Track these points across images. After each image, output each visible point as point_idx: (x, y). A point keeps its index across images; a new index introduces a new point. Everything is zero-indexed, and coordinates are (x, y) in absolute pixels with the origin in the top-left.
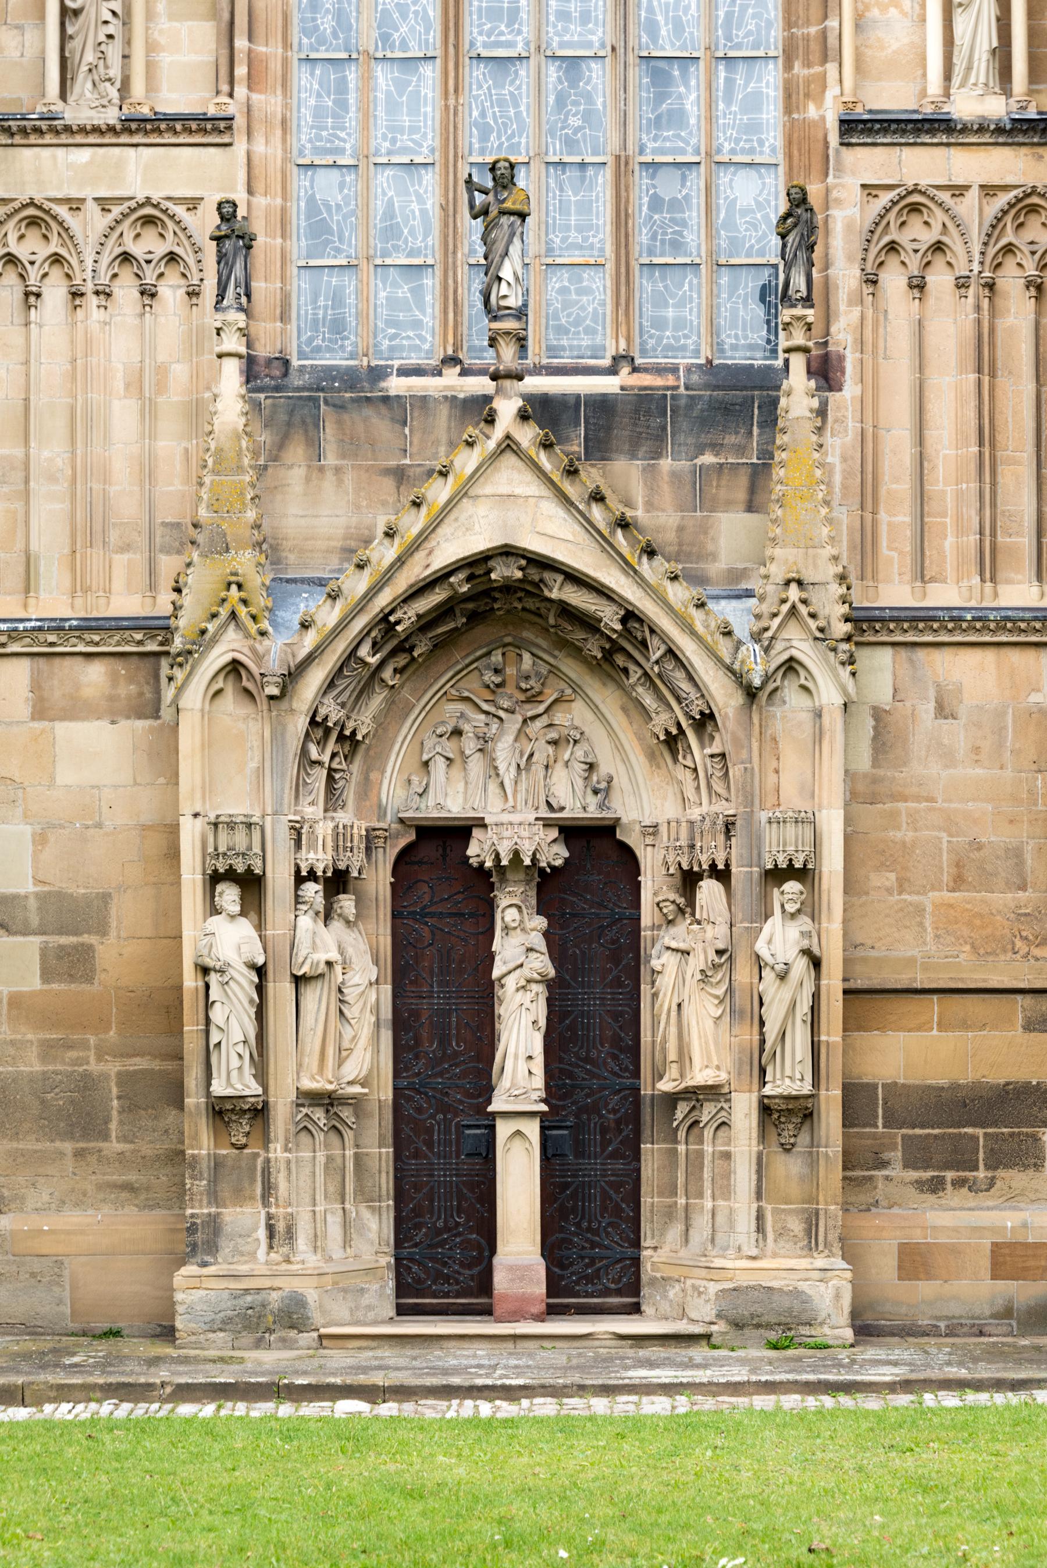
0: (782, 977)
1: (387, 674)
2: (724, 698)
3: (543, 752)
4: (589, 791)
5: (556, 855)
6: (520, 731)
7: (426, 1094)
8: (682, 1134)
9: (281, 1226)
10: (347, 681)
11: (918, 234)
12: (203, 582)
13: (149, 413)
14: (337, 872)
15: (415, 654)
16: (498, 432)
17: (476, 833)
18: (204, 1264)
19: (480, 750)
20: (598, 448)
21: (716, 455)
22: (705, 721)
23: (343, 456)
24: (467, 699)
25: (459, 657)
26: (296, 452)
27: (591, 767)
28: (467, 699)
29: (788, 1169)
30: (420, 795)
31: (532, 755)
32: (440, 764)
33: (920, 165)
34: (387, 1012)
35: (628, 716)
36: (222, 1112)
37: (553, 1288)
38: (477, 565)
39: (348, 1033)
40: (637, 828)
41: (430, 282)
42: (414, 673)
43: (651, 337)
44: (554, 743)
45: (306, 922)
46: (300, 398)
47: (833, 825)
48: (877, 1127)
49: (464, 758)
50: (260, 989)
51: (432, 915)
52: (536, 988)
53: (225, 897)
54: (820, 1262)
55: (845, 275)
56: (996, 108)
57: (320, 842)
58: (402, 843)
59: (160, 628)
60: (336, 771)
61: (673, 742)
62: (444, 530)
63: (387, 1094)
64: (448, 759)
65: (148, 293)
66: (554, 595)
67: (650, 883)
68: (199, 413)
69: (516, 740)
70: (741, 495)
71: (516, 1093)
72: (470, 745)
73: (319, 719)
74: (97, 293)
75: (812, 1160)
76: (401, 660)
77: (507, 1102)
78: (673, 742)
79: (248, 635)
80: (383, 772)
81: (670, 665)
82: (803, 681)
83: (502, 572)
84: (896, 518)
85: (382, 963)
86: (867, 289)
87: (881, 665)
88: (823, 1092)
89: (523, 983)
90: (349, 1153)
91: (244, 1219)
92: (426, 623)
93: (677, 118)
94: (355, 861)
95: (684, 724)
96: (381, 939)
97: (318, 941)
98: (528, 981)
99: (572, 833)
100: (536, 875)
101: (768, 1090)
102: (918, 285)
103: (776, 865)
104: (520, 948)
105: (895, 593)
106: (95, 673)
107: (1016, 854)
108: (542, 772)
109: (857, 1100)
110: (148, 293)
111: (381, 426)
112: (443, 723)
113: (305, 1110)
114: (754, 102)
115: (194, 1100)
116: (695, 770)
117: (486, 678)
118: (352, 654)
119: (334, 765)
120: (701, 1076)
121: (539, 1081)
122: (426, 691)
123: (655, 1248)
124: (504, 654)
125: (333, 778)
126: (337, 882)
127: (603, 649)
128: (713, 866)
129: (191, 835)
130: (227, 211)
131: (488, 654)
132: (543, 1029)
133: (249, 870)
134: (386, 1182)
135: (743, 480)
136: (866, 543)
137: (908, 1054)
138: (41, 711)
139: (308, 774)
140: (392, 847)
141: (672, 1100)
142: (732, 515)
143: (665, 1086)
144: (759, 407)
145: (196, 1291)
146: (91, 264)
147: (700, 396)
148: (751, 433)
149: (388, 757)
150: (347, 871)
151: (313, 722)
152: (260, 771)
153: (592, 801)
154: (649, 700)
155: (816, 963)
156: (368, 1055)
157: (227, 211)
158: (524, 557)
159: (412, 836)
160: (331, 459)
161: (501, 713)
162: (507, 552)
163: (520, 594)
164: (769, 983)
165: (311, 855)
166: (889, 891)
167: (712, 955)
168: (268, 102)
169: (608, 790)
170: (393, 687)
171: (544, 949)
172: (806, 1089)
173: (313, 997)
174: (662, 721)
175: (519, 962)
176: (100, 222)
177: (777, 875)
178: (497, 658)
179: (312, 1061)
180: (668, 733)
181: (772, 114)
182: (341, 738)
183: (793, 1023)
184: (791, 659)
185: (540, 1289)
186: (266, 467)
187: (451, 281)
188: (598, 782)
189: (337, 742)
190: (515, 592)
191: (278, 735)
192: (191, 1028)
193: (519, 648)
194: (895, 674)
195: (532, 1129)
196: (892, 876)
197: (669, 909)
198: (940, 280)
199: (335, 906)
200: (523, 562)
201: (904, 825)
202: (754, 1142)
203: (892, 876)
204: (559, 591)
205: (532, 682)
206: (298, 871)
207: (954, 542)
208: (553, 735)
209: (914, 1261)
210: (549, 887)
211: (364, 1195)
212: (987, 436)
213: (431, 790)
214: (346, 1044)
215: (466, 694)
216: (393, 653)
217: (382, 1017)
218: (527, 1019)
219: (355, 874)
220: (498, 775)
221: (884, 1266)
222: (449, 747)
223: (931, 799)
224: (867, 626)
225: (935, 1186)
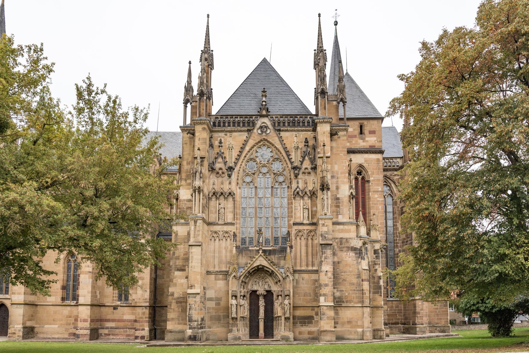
3: (264, 283)
5: (266, 293)
11: (300, 234)
12: (231, 268)
13: (226, 251)
20: (270, 254)
22: (279, 281)
25: (256, 274)
26: (241, 255)
29: (287, 324)
33: (301, 227)
36: (233, 318)
38: (258, 266)
47: (292, 291)
55: (293, 238)
56: (308, 222)
59: (228, 272)
65: (226, 240)
68: (231, 251)
84: (298, 261)
87: (297, 275)
91: (235, 329)
92: (253, 272)
93: (277, 223)
94: (246, 294)
99: (267, 291)
102: (300, 239)
104: (262, 302)
105: (298, 268)
106: (221, 276)
107: (310, 293)
109: (294, 317)
110: (226, 240)
111: (249, 252)
114: (285, 221)
115: (230, 317)
120: (279, 315)
126: (244, 296)
129: (230, 292)
130: (234, 233)
134: (248, 325)
136: (295, 263)
137: (299, 313)
138: (216, 280)
141: (276, 317)
145: (230, 336)
146: (221, 237)
157: (234, 233)
162: (261, 265)
164: (285, 306)
168: (238, 221)
173: (242, 308)
174: (275, 281)
176: (222, 233)
181: (286, 222)
191: (239, 282)
192: (230, 310)
195: (263, 320)
198: (302, 238)
207: (304, 263)
209: (300, 333)
210: (265, 296)
211: (246, 327)
212: (307, 253)
221: (297, 333)
224: (295, 271)
225: (302, 326)
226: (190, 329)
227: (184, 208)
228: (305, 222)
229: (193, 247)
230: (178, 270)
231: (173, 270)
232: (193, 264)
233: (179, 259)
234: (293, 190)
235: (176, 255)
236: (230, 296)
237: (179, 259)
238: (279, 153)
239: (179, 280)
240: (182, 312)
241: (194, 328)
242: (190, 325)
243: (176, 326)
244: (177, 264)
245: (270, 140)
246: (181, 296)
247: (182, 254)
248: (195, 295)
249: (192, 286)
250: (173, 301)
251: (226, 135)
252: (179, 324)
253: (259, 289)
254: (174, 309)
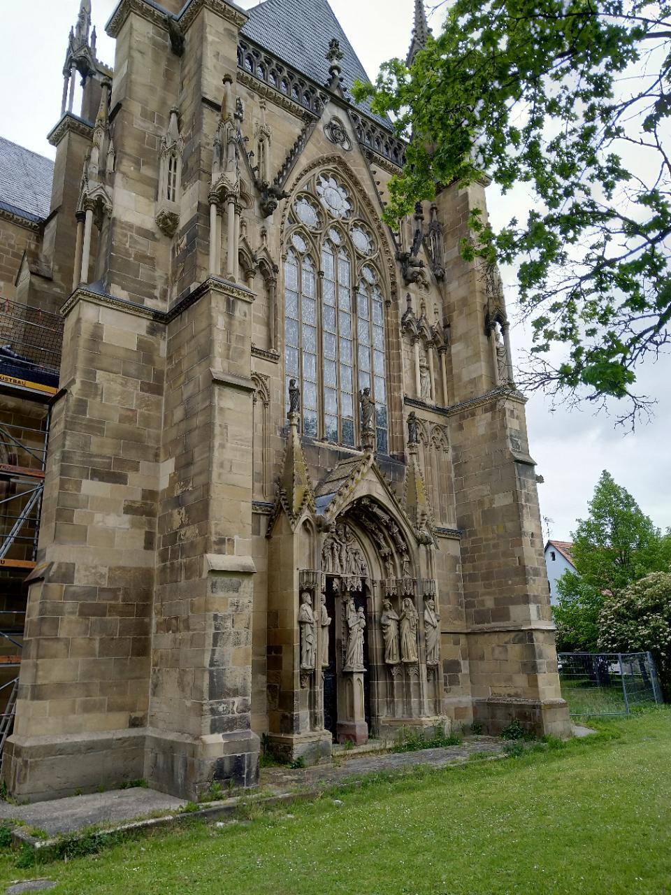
83: (365, 502)
101: (429, 662)
195: (362, 677)
226: (213, 730)
227: (129, 255)
228: (429, 402)
229: (228, 391)
230: (98, 475)
231: (75, 472)
232: (228, 454)
233: (101, 431)
234: (401, 316)
235: (93, 413)
237: (101, 431)
238: (368, 211)
239: (98, 517)
240: (101, 653)
241: (232, 724)
242: (213, 711)
243: (72, 717)
244: (94, 449)
245: (353, 169)
246: (105, 584)
247: (116, 418)
248: (235, 579)
249: (221, 542)
250: (69, 605)
251: (252, 97)
252: (88, 708)
254: (68, 642)
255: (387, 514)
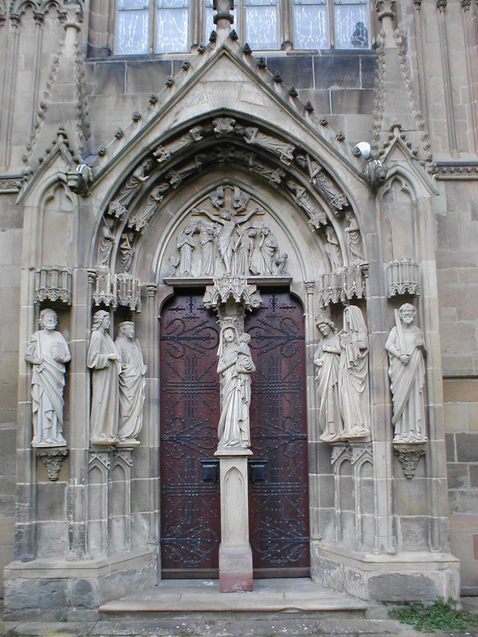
0: (406, 364)
1: (155, 193)
2: (357, 192)
3: (247, 242)
4: (274, 264)
6: (233, 231)
7: (180, 443)
8: (337, 469)
9: (76, 534)
10: (129, 191)
14: (120, 307)
15: (172, 182)
16: (218, 45)
17: (208, 288)
18: (25, 560)
19: (210, 241)
21: (340, 85)
22: (345, 212)
23: (137, 90)
24: (203, 214)
25: (198, 190)
26: (112, 89)
27: (275, 250)
28: (203, 214)
29: (410, 491)
30: (176, 267)
31: (240, 244)
32: (187, 248)
34: (155, 394)
35: (296, 221)
36: (40, 457)
37: (257, 562)
38: (205, 121)
39: (126, 406)
40: (302, 285)
41: (186, 16)
42: (171, 199)
43: (302, 38)
44: (253, 237)
45: (97, 334)
46: (115, 63)
48: (454, 461)
49: (202, 245)
50: (67, 377)
51: (184, 339)
52: (243, 377)
53: (45, 318)
54: (437, 556)
57: (109, 285)
58: (165, 295)
60: (124, 249)
61: (322, 231)
62: (188, 100)
63: (155, 444)
64: (192, 247)
66: (252, 140)
67: (311, 316)
69: (231, 235)
70: (355, 105)
71: (232, 443)
72: (204, 238)
73: (110, 213)
74: (12, 19)
75: (426, 486)
76: (164, 187)
77: (226, 449)
78: (322, 231)
79: (68, 163)
80: (154, 254)
81: (323, 178)
82: (404, 186)
83: (223, 126)
85: (152, 365)
86: (416, 7)
88: (433, 440)
89: (236, 374)
90: (128, 482)
95: (331, 218)
96: (151, 350)
97: (105, 347)
98: (239, 373)
99: (266, 288)
100: (244, 312)
101: (397, 439)
103: (397, 293)
104: (234, 354)
108: (246, 253)
112: (189, 227)
113: (95, 456)
115: (22, 450)
116: (338, 246)
117: (214, 201)
118: (131, 174)
119: (123, 246)
120: (353, 431)
121: (246, 436)
122: (179, 209)
123: (320, 540)
124: (224, 190)
125: (122, 254)
127: (281, 178)
128: (355, 297)
131: (214, 189)
132: (249, 403)
133: (59, 301)
135: (355, 98)
139: (103, 246)
140: (159, 297)
141: (329, 447)
142: (350, 115)
143: (326, 437)
144: (362, 62)
147: (330, 58)
148: (358, 75)
149: (157, 245)
150: (127, 308)
151: (106, 215)
152: (72, 244)
153: (276, 270)
154: (309, 206)
155: (425, 355)
156: (140, 420)
158: (234, 118)
159: (170, 291)
160: (130, 92)
161: (223, 221)
162: (224, 113)
163: (233, 148)
164: (396, 370)
165: (103, 293)
166: (453, 318)
167: (357, 352)
169: (285, 262)
170: (158, 202)
171: (249, 353)
172: (424, 439)
173: (102, 383)
174: (317, 218)
175: (234, 362)
177: (397, 300)
178: (220, 191)
179: (98, 422)
180: (321, 224)
182: (127, 230)
183: (414, 396)
184: (397, 173)
185: (249, 570)
186: (95, 97)
187: (196, 11)
188: (279, 258)
189: (123, 233)
190: (230, 147)
193: (232, 185)
194: (447, 196)
195: (243, 466)
196: (455, 309)
197: (325, 329)
199: (121, 328)
200: (234, 121)
201: (459, 280)
202: (389, 474)
203: (455, 309)
204: (255, 138)
205: (240, 203)
206: (94, 303)
208: (252, 232)
213: (181, 264)
214: (124, 413)
215: (202, 211)
216: (157, 183)
217: (152, 397)
218: (238, 397)
219: (133, 309)
220: (221, 255)
222: (193, 241)
223: (473, 265)
236: (27, 307)
253: (217, 273)
255: (286, 141)
